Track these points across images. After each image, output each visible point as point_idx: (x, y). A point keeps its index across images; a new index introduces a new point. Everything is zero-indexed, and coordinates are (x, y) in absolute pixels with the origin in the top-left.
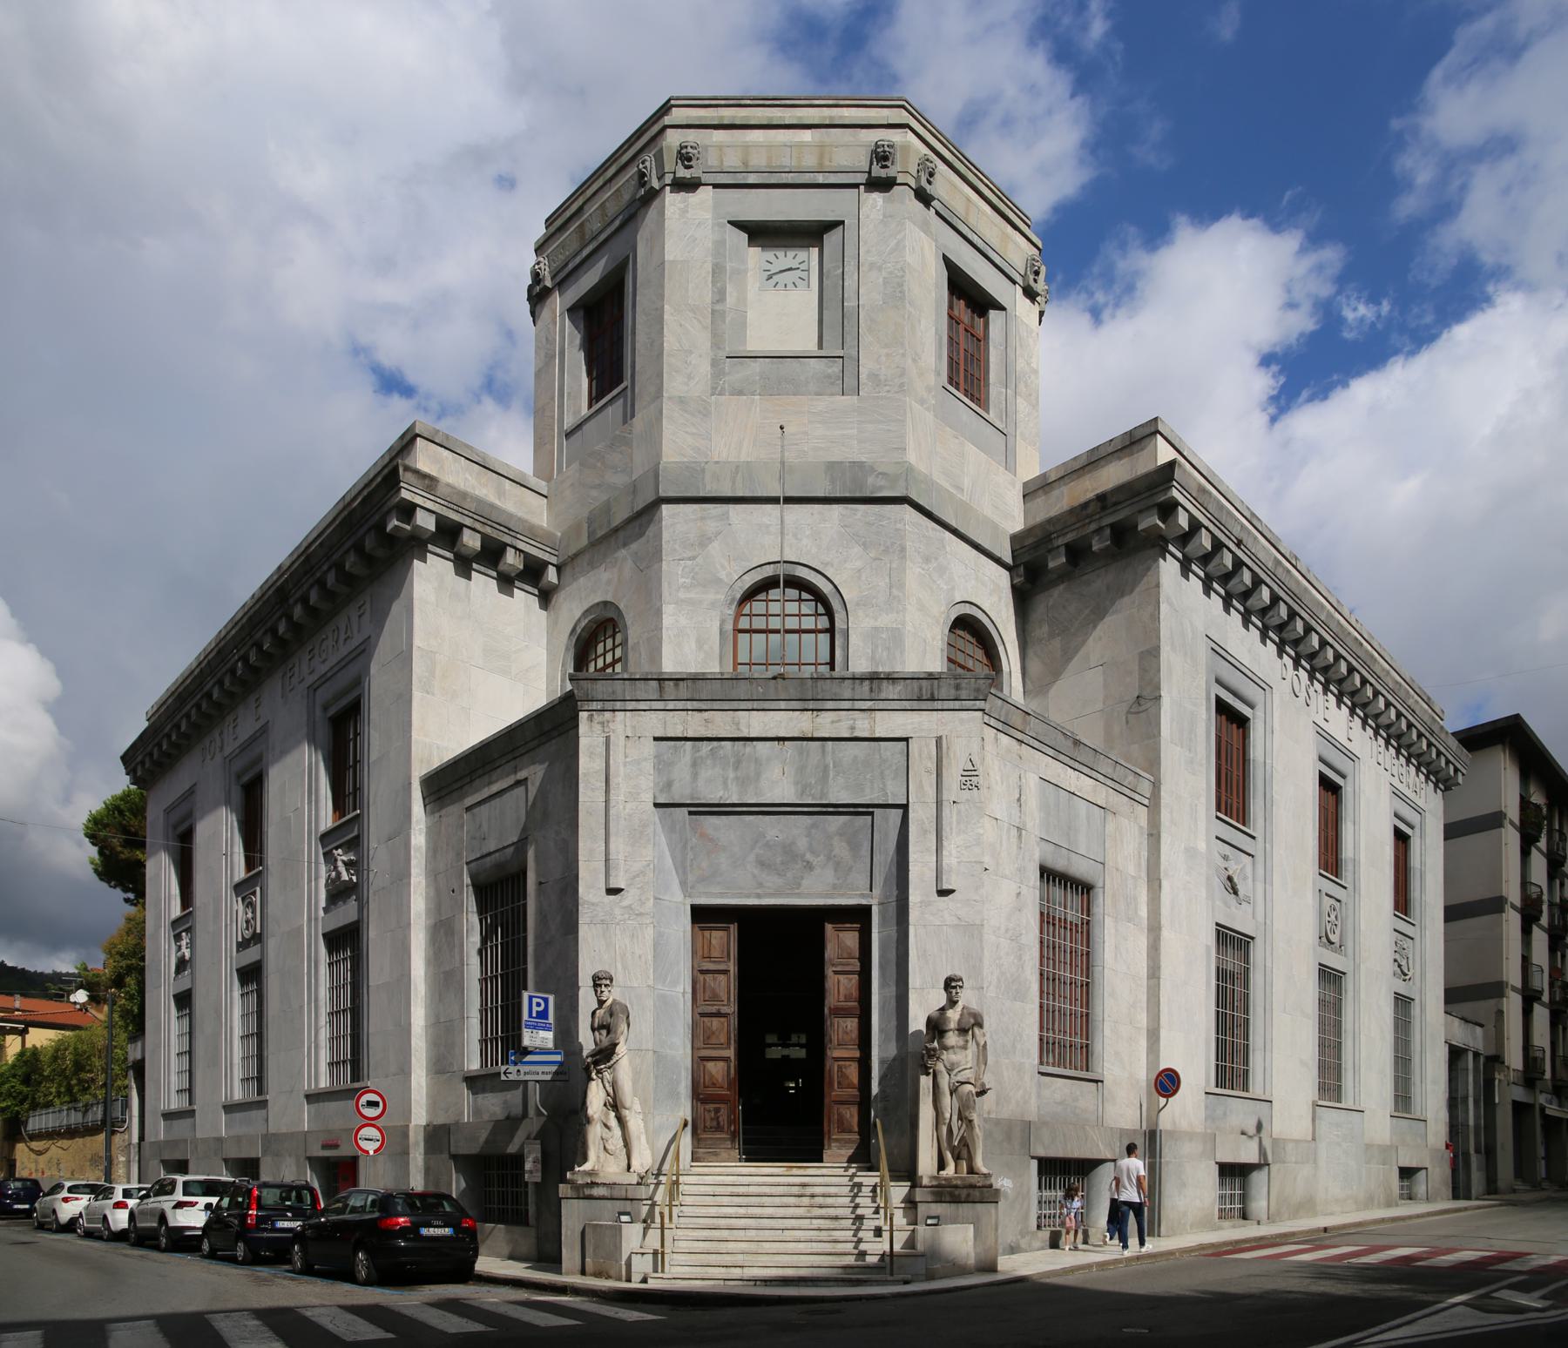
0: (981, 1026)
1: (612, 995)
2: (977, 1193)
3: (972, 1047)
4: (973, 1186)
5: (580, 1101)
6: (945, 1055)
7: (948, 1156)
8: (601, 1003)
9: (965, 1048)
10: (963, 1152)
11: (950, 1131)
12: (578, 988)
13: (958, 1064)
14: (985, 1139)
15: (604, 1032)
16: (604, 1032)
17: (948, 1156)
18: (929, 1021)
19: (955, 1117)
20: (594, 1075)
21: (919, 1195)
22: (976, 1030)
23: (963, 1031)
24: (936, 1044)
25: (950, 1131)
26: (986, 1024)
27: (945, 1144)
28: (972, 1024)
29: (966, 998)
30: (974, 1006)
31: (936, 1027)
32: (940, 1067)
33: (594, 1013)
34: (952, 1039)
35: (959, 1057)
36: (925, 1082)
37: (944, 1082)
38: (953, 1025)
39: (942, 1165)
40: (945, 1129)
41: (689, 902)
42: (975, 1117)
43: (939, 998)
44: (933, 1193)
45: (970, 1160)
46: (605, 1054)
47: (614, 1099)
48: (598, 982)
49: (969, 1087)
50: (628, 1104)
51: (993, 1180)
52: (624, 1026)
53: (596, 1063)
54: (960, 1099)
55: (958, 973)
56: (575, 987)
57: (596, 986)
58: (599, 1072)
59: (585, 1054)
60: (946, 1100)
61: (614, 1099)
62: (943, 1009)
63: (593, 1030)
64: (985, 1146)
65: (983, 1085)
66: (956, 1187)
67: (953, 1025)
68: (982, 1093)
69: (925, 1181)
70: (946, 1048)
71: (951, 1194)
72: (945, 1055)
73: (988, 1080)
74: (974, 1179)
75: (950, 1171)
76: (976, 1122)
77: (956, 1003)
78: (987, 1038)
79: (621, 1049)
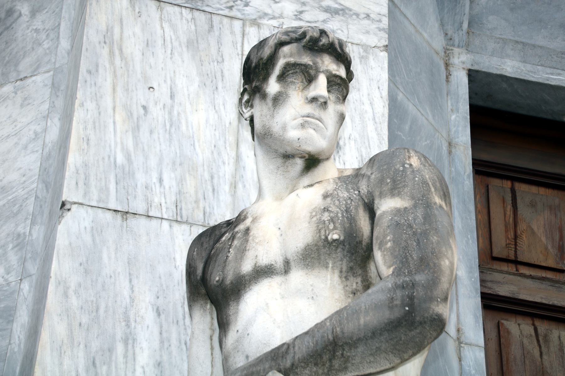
41: (462, 61)
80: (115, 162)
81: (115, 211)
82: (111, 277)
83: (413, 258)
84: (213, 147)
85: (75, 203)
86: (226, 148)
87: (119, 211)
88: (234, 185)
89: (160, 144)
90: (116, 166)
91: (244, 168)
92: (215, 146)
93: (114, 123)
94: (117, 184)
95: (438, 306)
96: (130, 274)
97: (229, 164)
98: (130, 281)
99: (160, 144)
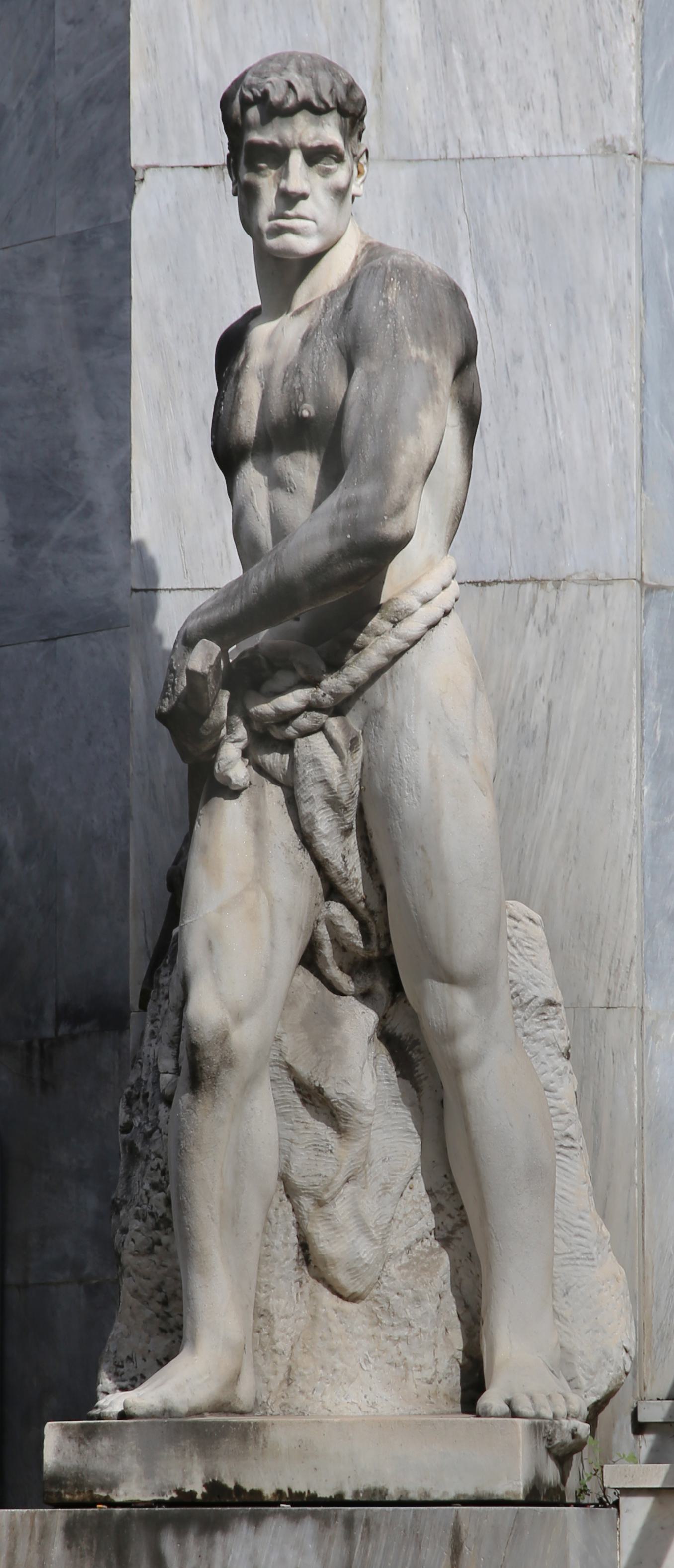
1: (342, 222)
5: (138, 939)
8: (283, 274)
12: (128, 180)
15: (303, 469)
16: (303, 469)
20: (232, 763)
33: (231, 347)
46: (319, 616)
47: (374, 918)
48: (252, 131)
50: (466, 953)
52: (435, 424)
53: (249, 678)
56: (108, 173)
57: (247, 158)
58: (268, 737)
59: (172, 617)
61: (374, 918)
63: (229, 456)
79: (419, 578)
80: (197, 79)
81: (206, 167)
82: (211, 279)
83: (365, 461)
84: (342, 10)
85: (147, 168)
86: (362, 8)
87: (211, 167)
88: (379, 77)
89: (261, 29)
90: (199, 87)
91: (394, 39)
92: (345, 10)
93: (189, 8)
94: (203, 119)
95: (384, 526)
96: (237, 269)
97: (369, 38)
98: (239, 281)
99: (261, 29)
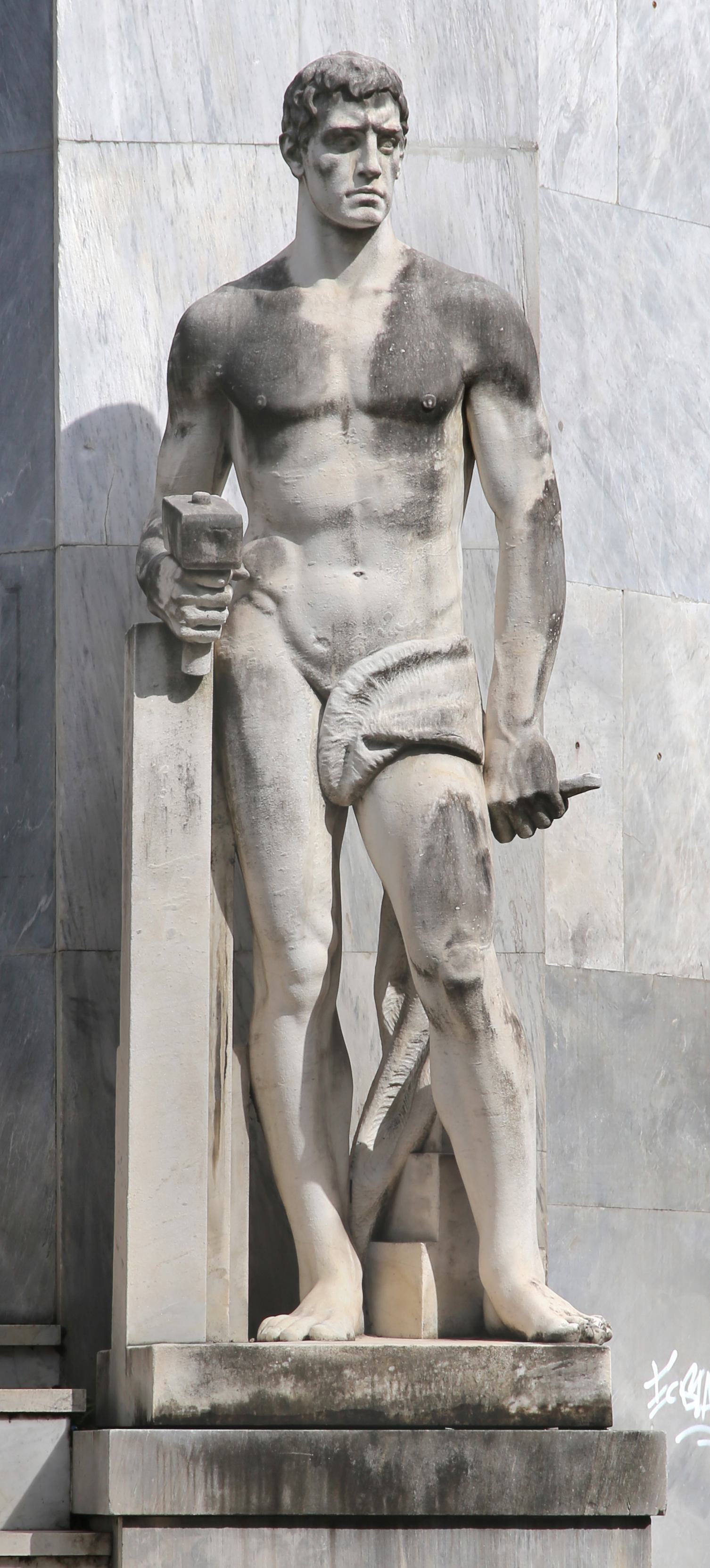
0: (520, 387)
2: (503, 1467)
3: (465, 520)
4: (480, 1418)
6: (292, 571)
7: (320, 1217)
9: (419, 522)
10: (416, 1185)
11: (330, 1050)
13: (378, 626)
14: (557, 1105)
17: (320, 1217)
18: (189, 348)
19: (361, 968)
21: (131, 1473)
22: (491, 409)
23: (406, 415)
24: (231, 498)
25: (330, 1050)
26: (554, 379)
27: (294, 1140)
28: (462, 378)
29: (428, 202)
30: (480, 263)
31: (231, 388)
32: (261, 641)
34: (335, 463)
35: (370, 589)
36: (167, 737)
37: (290, 740)
38: (340, 377)
39: (276, 1281)
40: (291, 1043)
42: (485, 962)
43: (265, 211)
44: (219, 1461)
45: (462, 1235)
49: (448, 775)
51: (611, 1378)
54: (391, 849)
55: (372, 48)
60: (302, 856)
62: (274, 277)
64: (556, 1153)
65: (538, 759)
66: (372, 1419)
67: (340, 377)
68: (534, 810)
69: (170, 1384)
70: (298, 525)
71: (341, 1468)
72: (292, 571)
73: (572, 729)
74: (488, 1370)
75: (328, 1314)
76: (496, 997)
77: (359, 236)
78: (565, 466)
